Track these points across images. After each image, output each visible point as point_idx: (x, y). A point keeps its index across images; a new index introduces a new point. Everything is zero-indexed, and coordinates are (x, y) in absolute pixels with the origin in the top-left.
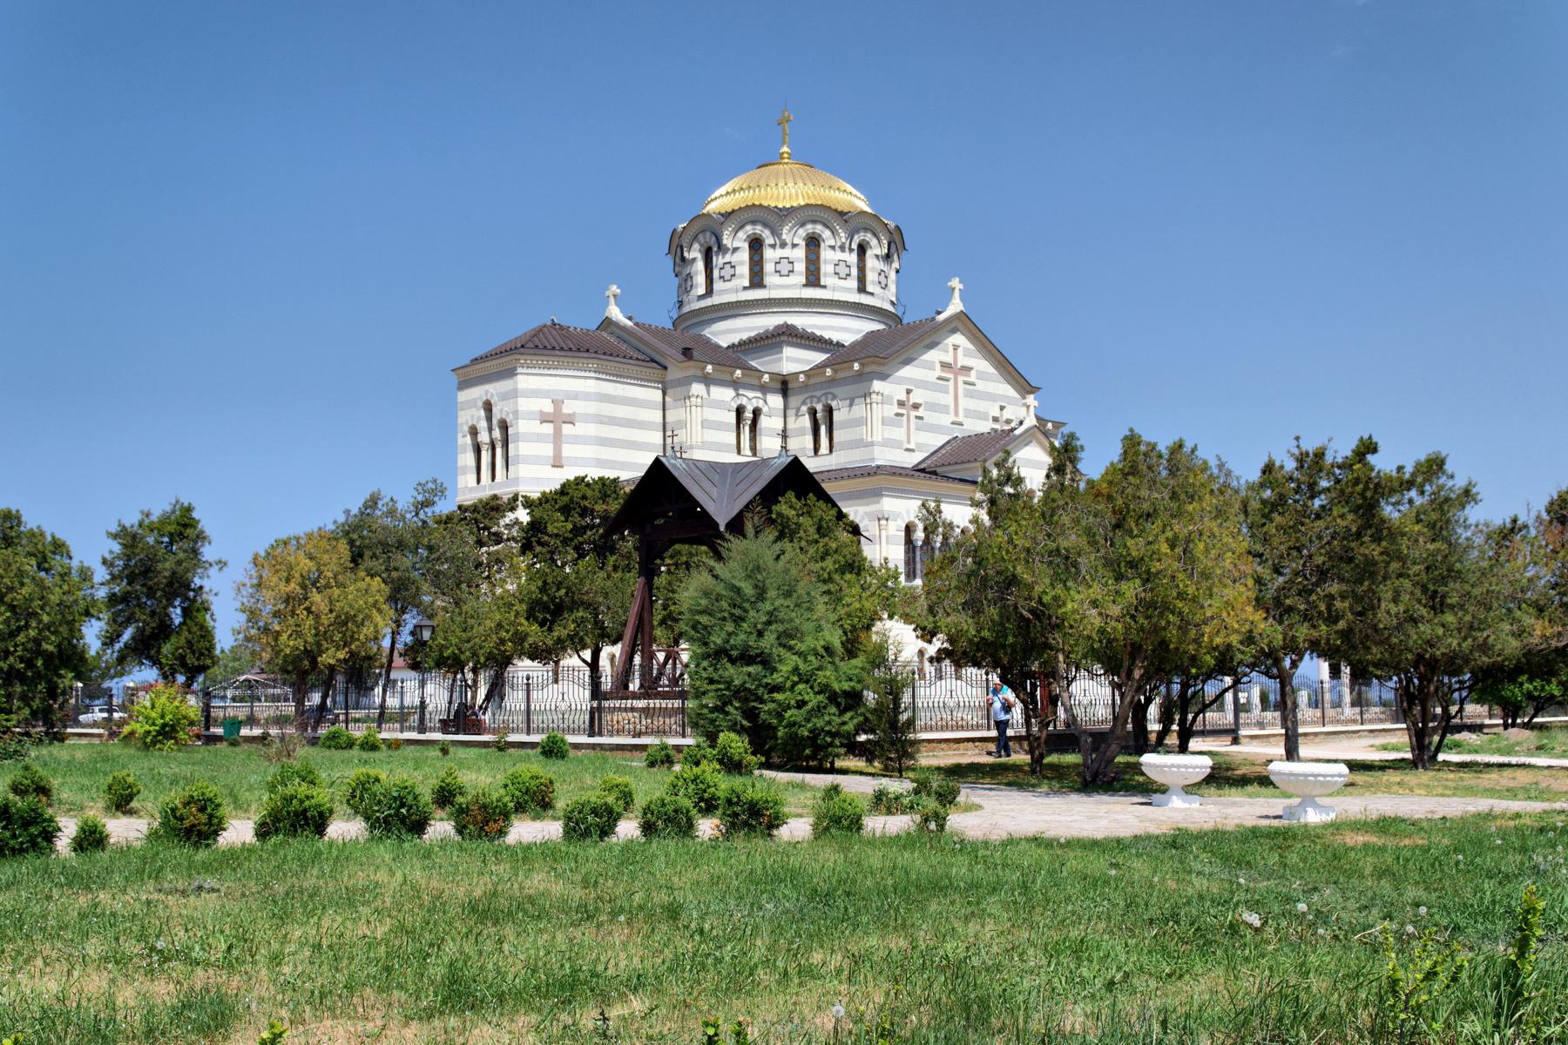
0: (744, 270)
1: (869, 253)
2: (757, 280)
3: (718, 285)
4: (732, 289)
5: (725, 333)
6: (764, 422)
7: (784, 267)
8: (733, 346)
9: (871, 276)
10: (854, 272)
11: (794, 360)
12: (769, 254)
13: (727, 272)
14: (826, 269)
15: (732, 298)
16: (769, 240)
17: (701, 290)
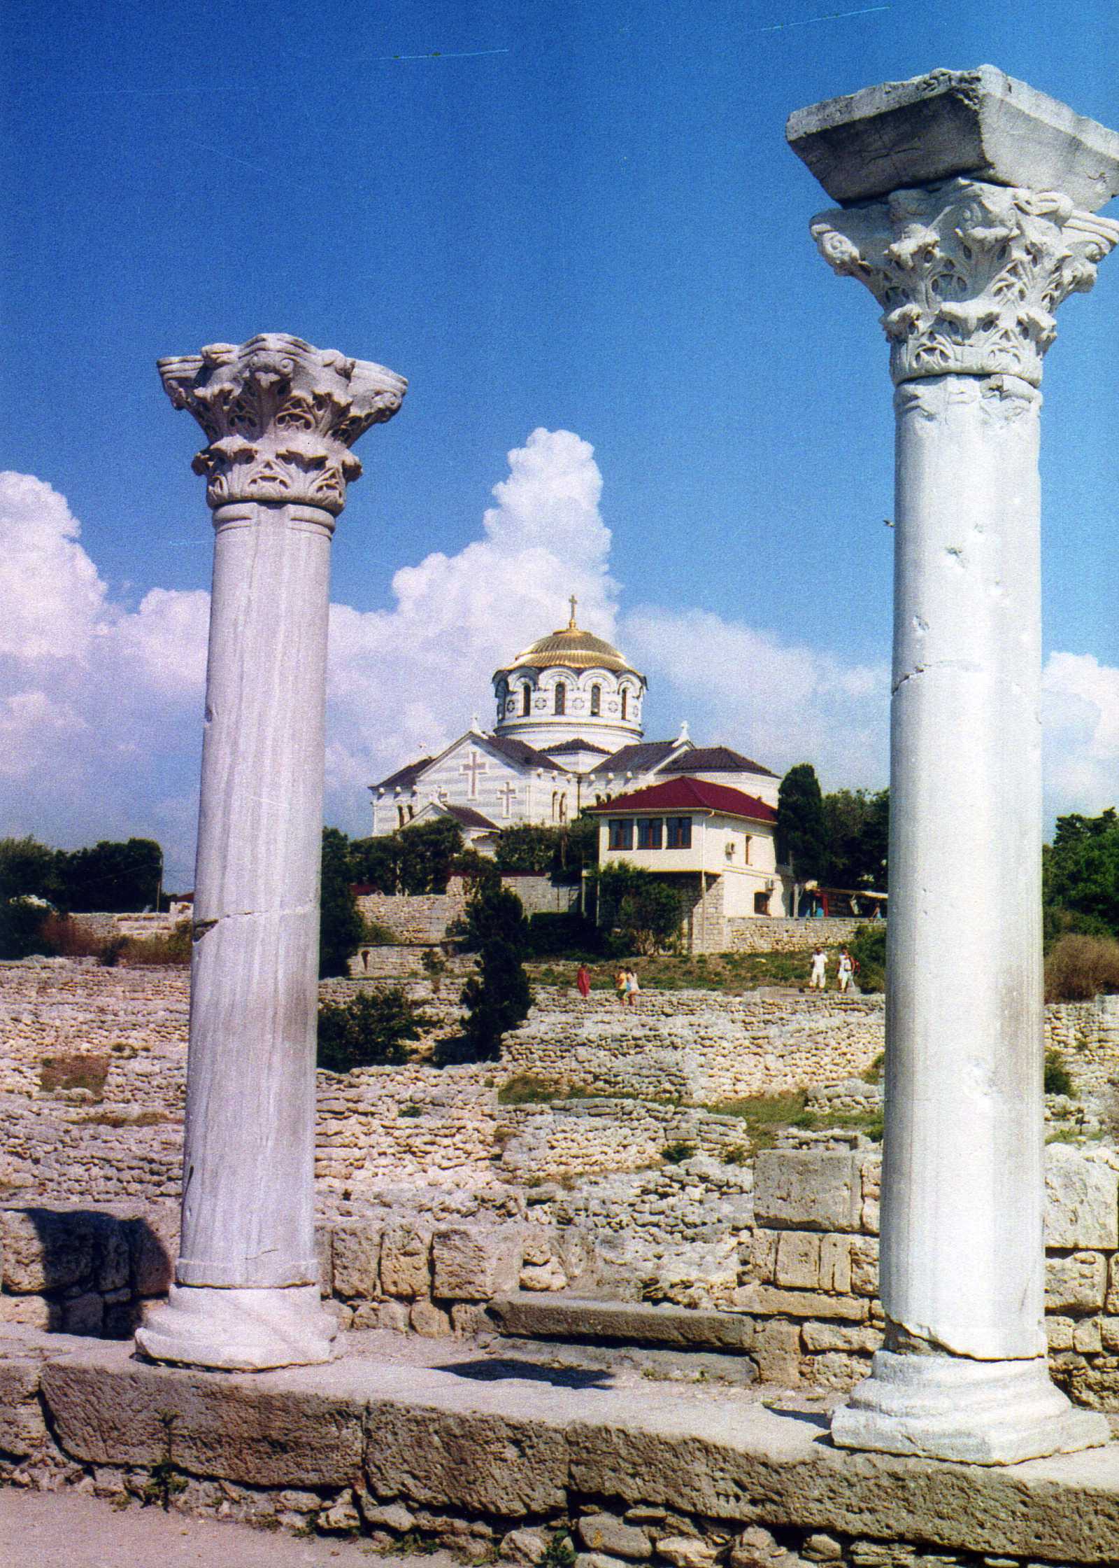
0: (551, 704)
1: (629, 696)
2: (560, 710)
3: (532, 711)
4: (543, 711)
5: (538, 741)
6: (567, 801)
7: (579, 704)
8: (544, 751)
9: (629, 710)
10: (620, 708)
11: (586, 762)
12: (569, 696)
13: (540, 704)
14: (604, 706)
15: (544, 720)
16: (568, 688)
17: (521, 712)
